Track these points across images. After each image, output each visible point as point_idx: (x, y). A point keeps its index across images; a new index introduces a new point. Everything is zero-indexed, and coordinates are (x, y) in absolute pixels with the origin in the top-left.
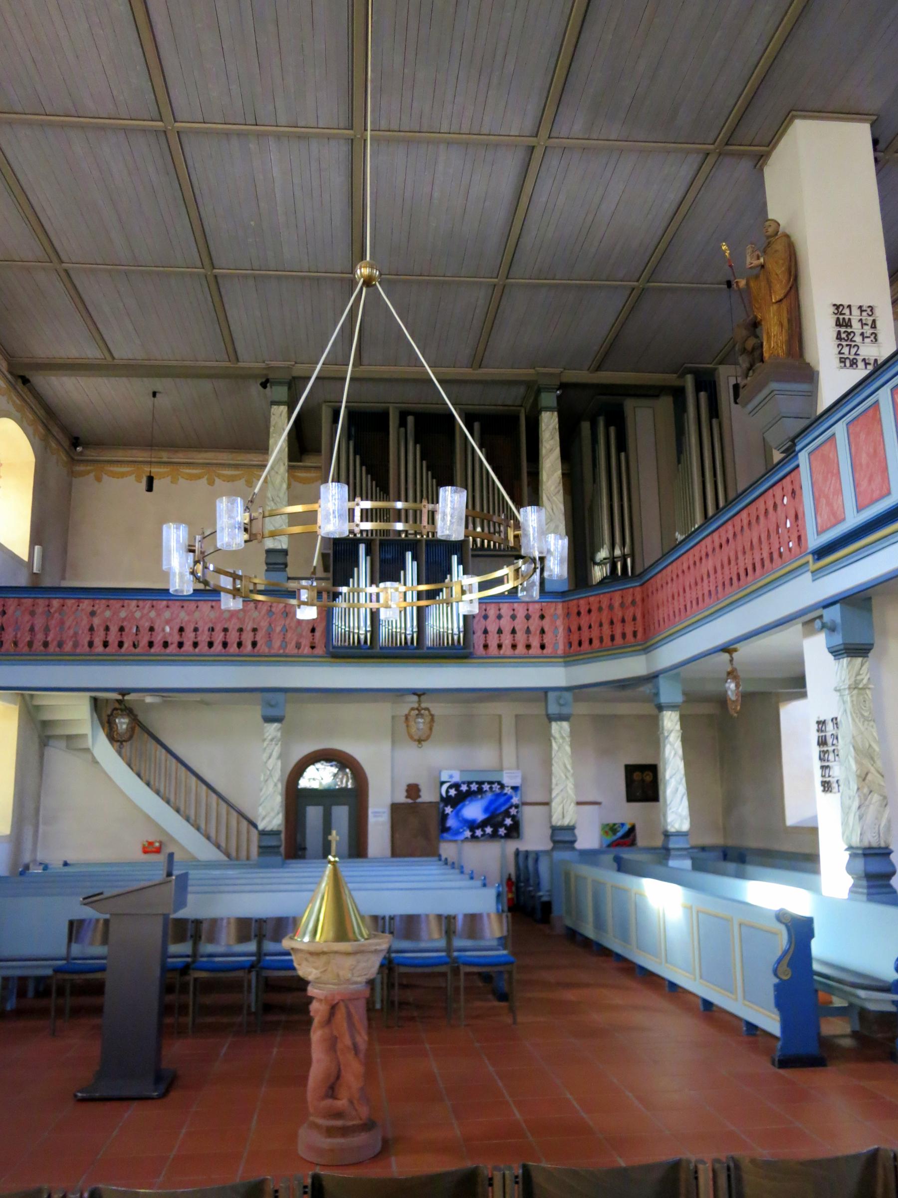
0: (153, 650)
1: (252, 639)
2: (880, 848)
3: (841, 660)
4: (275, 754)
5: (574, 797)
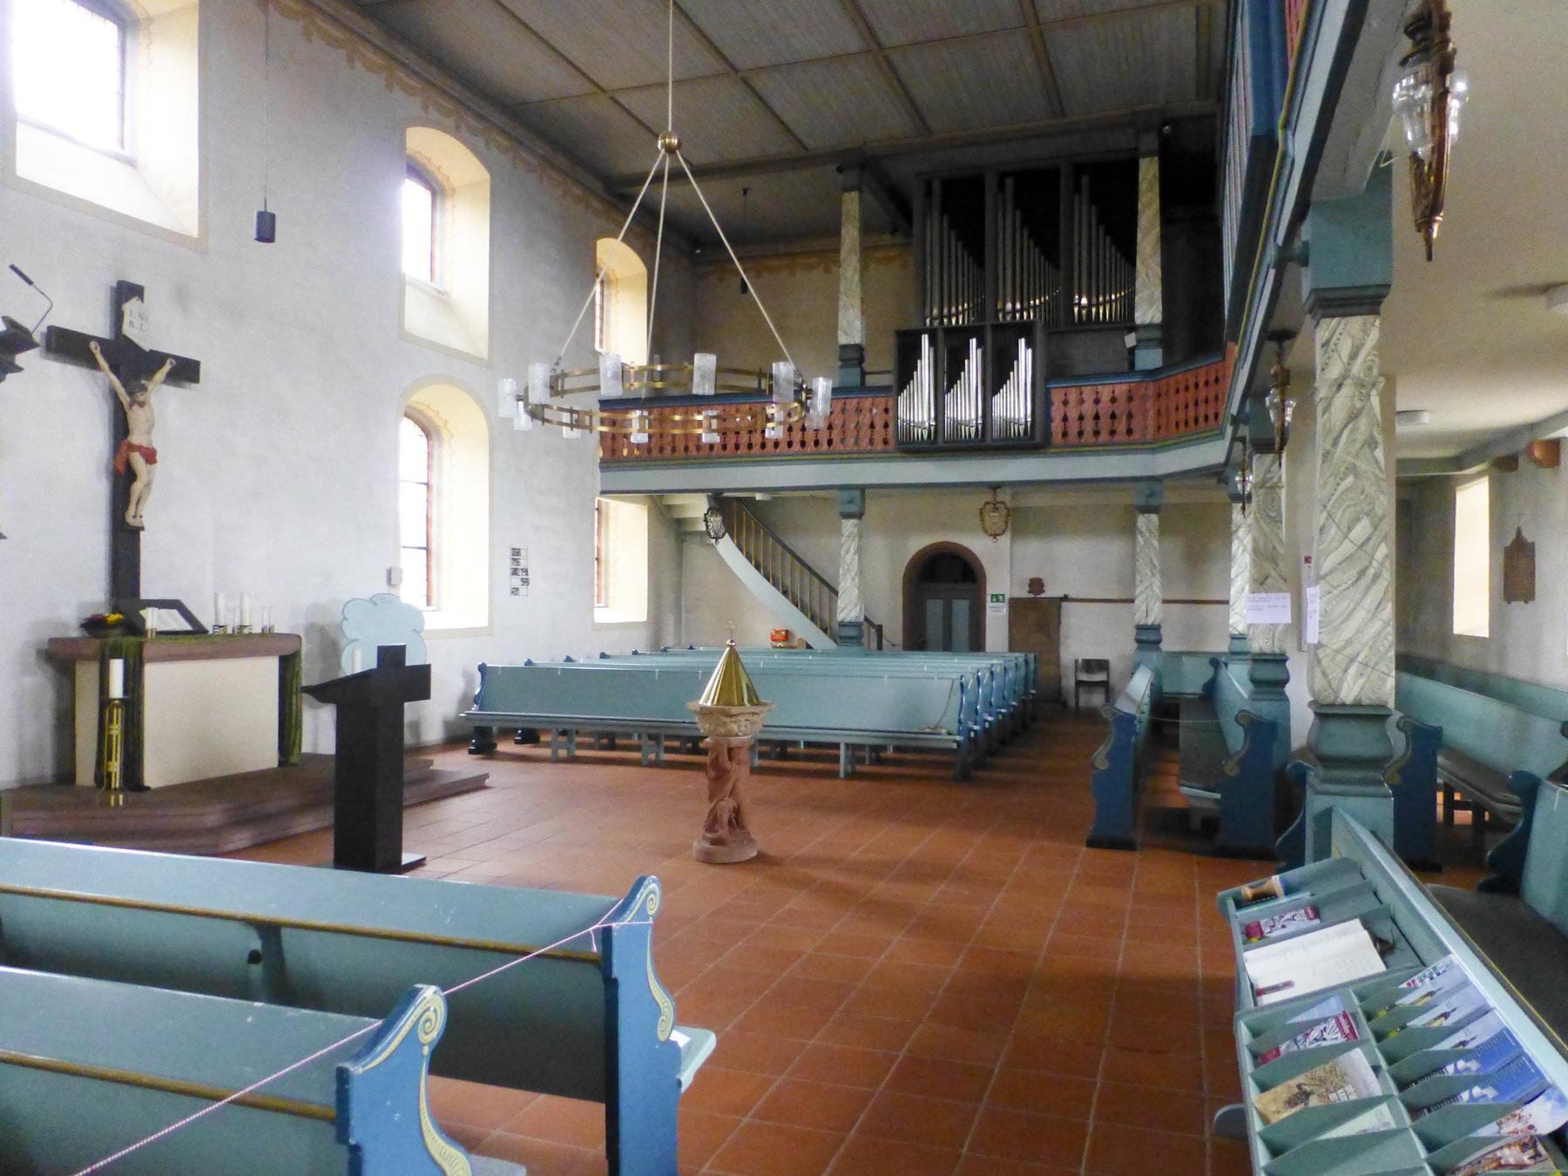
0: (739, 452)
1: (828, 437)
2: (1275, 654)
3: (1264, 456)
4: (852, 550)
5: (1160, 595)
